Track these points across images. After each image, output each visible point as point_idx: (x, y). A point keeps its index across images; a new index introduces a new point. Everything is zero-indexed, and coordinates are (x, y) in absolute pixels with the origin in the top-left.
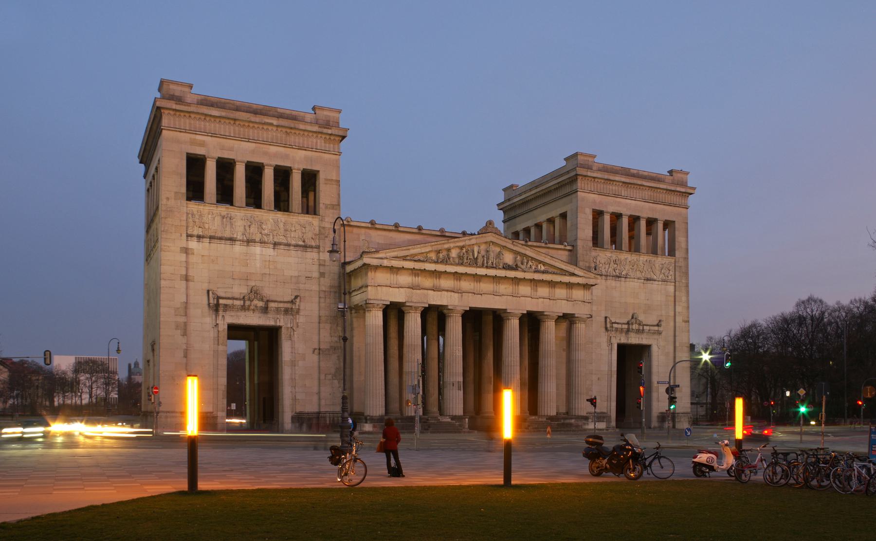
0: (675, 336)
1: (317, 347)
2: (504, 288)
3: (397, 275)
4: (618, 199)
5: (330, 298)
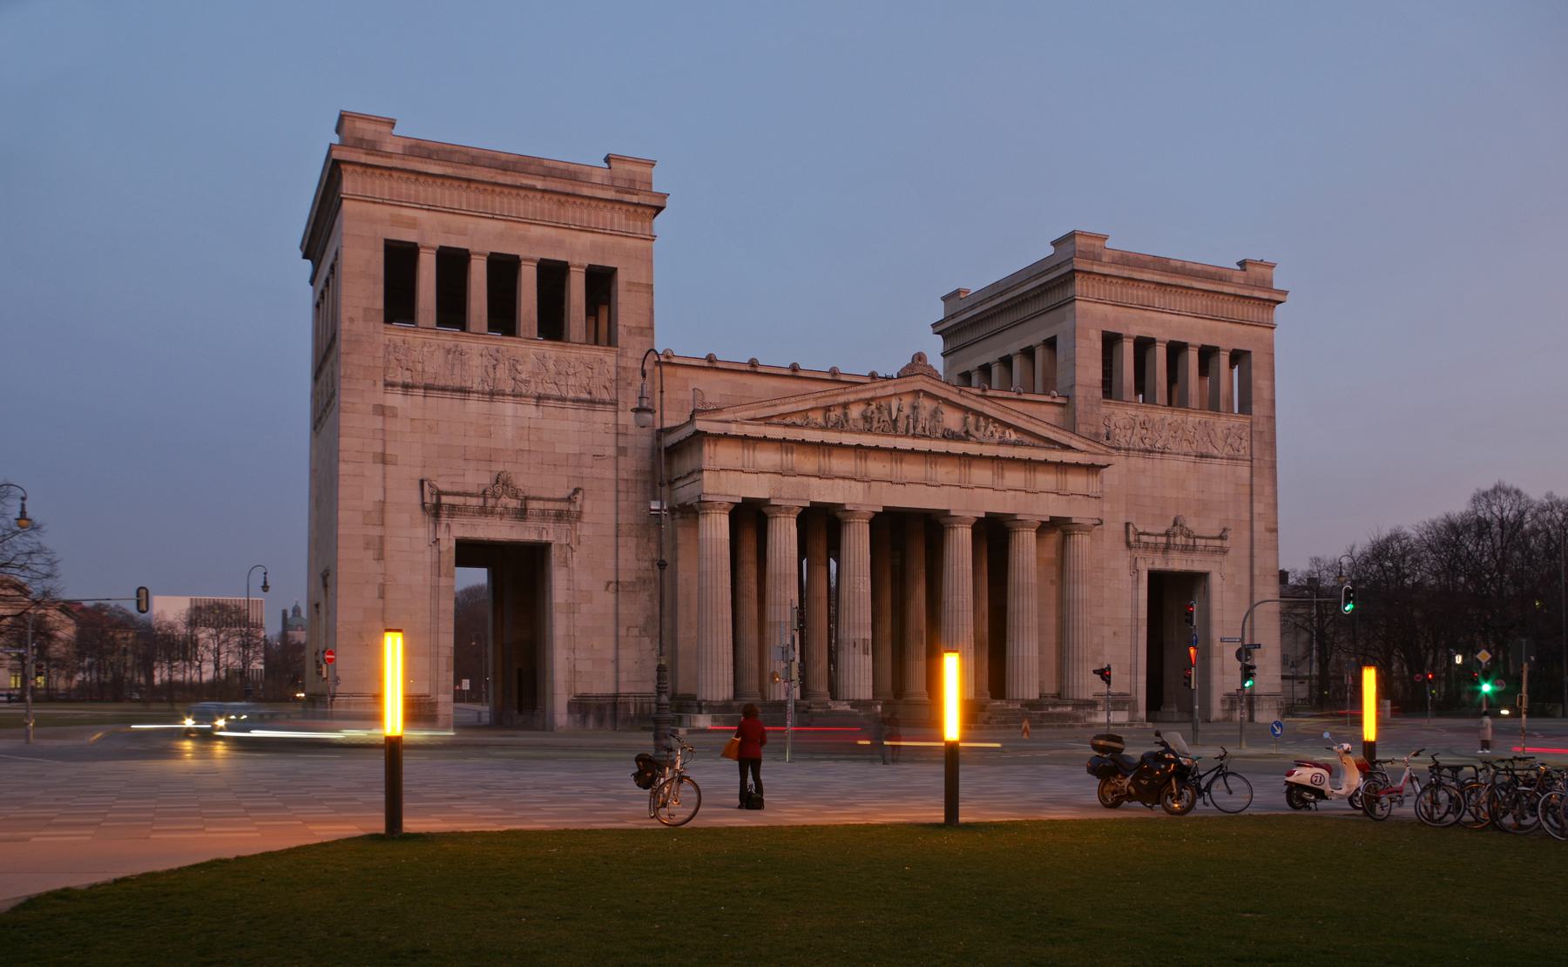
0: (1252, 556)
1: (613, 579)
2: (944, 472)
3: (754, 450)
4: (1148, 314)
5: (636, 493)
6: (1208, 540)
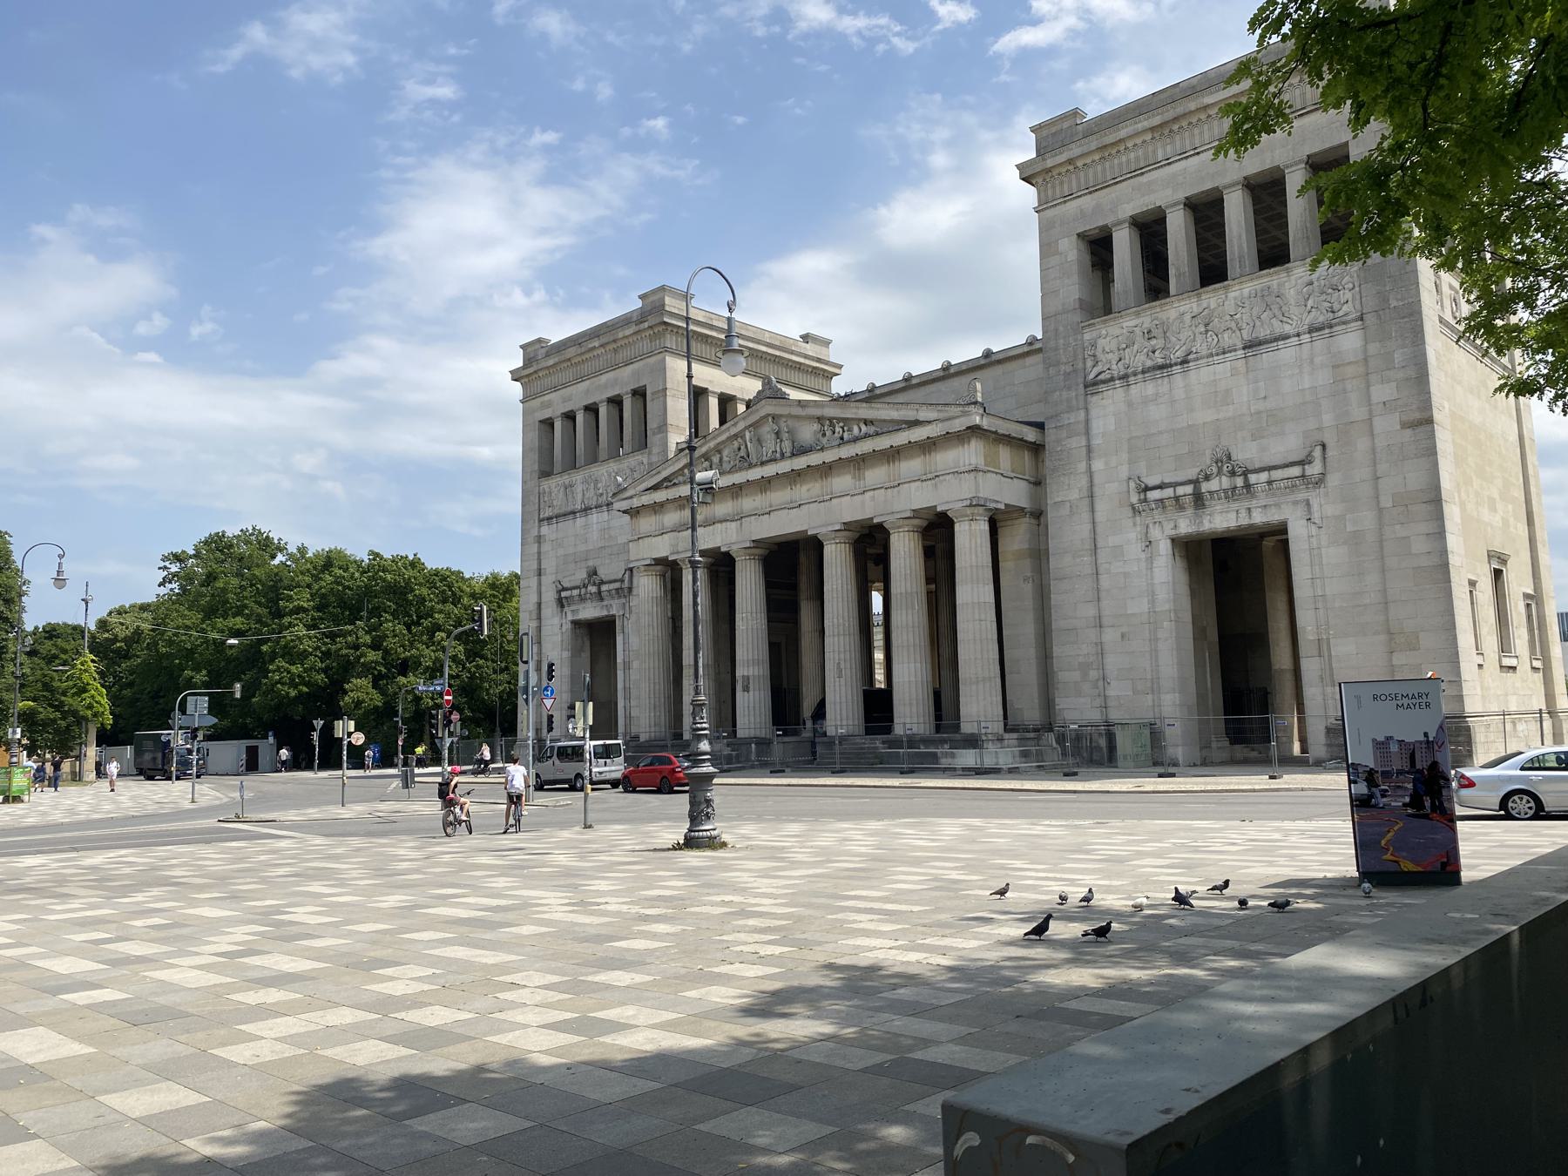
6: (1273, 472)
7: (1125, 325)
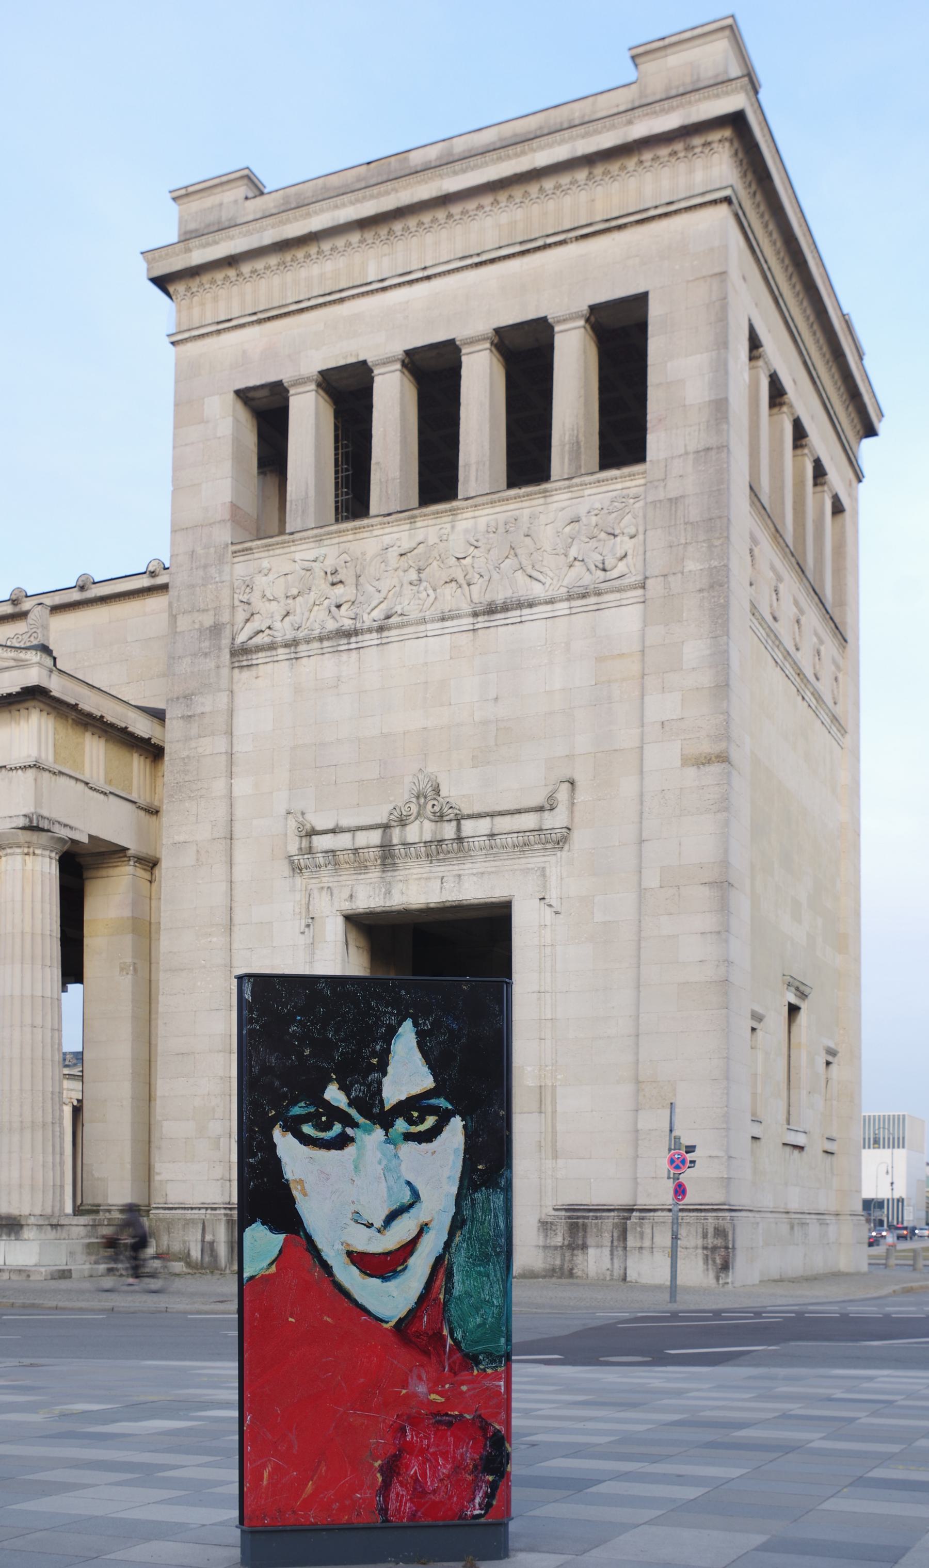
6: (498, 820)
7: (298, 556)
